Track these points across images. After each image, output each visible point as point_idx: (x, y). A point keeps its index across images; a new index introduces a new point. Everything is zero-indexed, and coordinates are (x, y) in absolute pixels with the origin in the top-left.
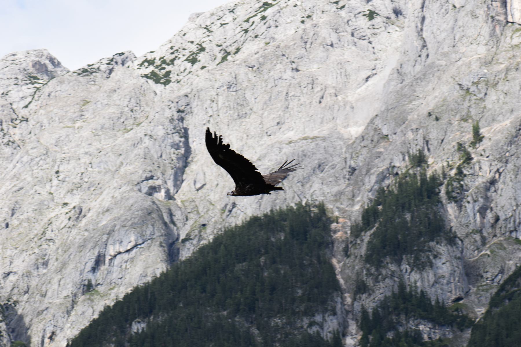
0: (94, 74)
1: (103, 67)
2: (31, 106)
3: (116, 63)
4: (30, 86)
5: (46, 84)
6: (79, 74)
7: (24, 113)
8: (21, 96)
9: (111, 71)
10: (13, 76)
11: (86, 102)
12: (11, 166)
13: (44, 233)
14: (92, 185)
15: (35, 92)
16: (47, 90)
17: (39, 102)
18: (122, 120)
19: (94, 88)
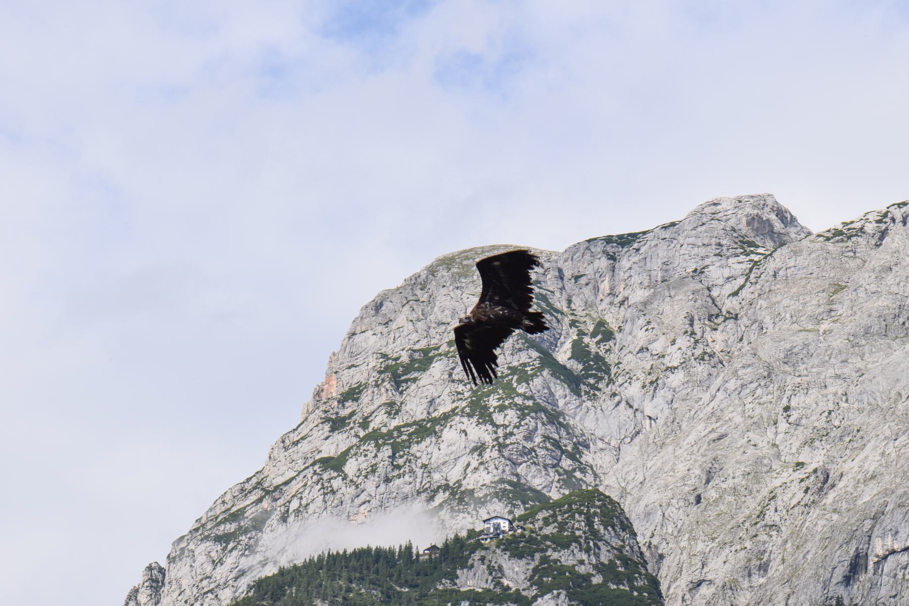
0: (853, 239)
1: (870, 228)
2: (744, 293)
3: (893, 220)
4: (742, 258)
5: (771, 255)
6: (828, 239)
7: (730, 304)
8: (726, 276)
9: (883, 234)
10: (713, 241)
11: (839, 288)
12: (706, 397)
13: (762, 515)
14: (846, 432)
15: (751, 270)
16: (771, 266)
17: (758, 286)
18: (901, 320)
19: (852, 264)
